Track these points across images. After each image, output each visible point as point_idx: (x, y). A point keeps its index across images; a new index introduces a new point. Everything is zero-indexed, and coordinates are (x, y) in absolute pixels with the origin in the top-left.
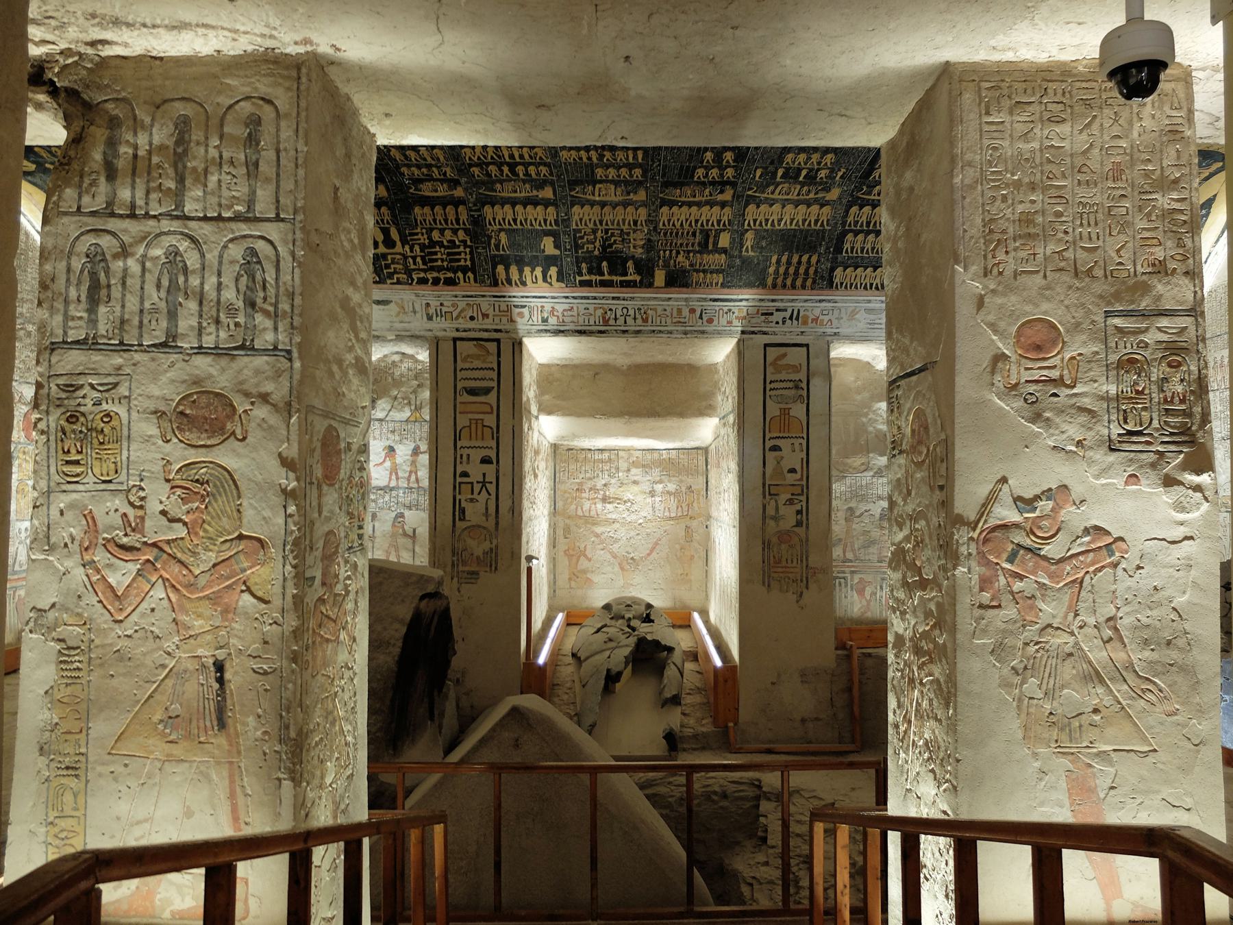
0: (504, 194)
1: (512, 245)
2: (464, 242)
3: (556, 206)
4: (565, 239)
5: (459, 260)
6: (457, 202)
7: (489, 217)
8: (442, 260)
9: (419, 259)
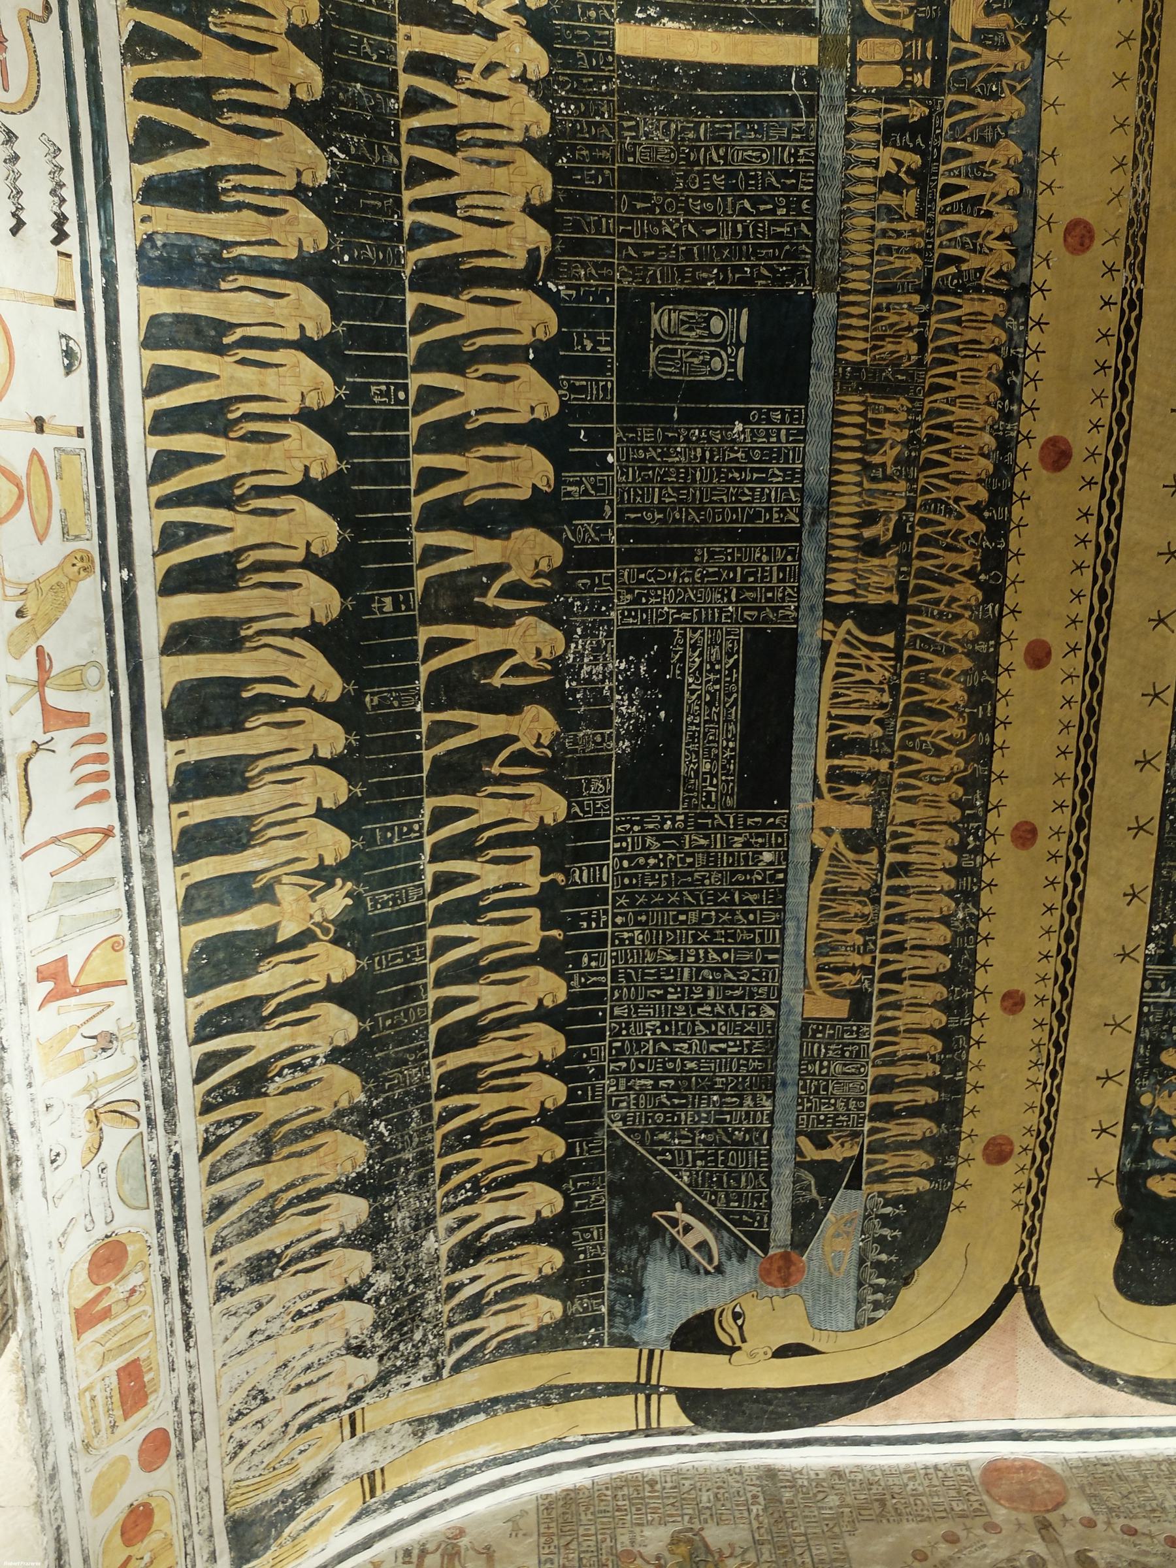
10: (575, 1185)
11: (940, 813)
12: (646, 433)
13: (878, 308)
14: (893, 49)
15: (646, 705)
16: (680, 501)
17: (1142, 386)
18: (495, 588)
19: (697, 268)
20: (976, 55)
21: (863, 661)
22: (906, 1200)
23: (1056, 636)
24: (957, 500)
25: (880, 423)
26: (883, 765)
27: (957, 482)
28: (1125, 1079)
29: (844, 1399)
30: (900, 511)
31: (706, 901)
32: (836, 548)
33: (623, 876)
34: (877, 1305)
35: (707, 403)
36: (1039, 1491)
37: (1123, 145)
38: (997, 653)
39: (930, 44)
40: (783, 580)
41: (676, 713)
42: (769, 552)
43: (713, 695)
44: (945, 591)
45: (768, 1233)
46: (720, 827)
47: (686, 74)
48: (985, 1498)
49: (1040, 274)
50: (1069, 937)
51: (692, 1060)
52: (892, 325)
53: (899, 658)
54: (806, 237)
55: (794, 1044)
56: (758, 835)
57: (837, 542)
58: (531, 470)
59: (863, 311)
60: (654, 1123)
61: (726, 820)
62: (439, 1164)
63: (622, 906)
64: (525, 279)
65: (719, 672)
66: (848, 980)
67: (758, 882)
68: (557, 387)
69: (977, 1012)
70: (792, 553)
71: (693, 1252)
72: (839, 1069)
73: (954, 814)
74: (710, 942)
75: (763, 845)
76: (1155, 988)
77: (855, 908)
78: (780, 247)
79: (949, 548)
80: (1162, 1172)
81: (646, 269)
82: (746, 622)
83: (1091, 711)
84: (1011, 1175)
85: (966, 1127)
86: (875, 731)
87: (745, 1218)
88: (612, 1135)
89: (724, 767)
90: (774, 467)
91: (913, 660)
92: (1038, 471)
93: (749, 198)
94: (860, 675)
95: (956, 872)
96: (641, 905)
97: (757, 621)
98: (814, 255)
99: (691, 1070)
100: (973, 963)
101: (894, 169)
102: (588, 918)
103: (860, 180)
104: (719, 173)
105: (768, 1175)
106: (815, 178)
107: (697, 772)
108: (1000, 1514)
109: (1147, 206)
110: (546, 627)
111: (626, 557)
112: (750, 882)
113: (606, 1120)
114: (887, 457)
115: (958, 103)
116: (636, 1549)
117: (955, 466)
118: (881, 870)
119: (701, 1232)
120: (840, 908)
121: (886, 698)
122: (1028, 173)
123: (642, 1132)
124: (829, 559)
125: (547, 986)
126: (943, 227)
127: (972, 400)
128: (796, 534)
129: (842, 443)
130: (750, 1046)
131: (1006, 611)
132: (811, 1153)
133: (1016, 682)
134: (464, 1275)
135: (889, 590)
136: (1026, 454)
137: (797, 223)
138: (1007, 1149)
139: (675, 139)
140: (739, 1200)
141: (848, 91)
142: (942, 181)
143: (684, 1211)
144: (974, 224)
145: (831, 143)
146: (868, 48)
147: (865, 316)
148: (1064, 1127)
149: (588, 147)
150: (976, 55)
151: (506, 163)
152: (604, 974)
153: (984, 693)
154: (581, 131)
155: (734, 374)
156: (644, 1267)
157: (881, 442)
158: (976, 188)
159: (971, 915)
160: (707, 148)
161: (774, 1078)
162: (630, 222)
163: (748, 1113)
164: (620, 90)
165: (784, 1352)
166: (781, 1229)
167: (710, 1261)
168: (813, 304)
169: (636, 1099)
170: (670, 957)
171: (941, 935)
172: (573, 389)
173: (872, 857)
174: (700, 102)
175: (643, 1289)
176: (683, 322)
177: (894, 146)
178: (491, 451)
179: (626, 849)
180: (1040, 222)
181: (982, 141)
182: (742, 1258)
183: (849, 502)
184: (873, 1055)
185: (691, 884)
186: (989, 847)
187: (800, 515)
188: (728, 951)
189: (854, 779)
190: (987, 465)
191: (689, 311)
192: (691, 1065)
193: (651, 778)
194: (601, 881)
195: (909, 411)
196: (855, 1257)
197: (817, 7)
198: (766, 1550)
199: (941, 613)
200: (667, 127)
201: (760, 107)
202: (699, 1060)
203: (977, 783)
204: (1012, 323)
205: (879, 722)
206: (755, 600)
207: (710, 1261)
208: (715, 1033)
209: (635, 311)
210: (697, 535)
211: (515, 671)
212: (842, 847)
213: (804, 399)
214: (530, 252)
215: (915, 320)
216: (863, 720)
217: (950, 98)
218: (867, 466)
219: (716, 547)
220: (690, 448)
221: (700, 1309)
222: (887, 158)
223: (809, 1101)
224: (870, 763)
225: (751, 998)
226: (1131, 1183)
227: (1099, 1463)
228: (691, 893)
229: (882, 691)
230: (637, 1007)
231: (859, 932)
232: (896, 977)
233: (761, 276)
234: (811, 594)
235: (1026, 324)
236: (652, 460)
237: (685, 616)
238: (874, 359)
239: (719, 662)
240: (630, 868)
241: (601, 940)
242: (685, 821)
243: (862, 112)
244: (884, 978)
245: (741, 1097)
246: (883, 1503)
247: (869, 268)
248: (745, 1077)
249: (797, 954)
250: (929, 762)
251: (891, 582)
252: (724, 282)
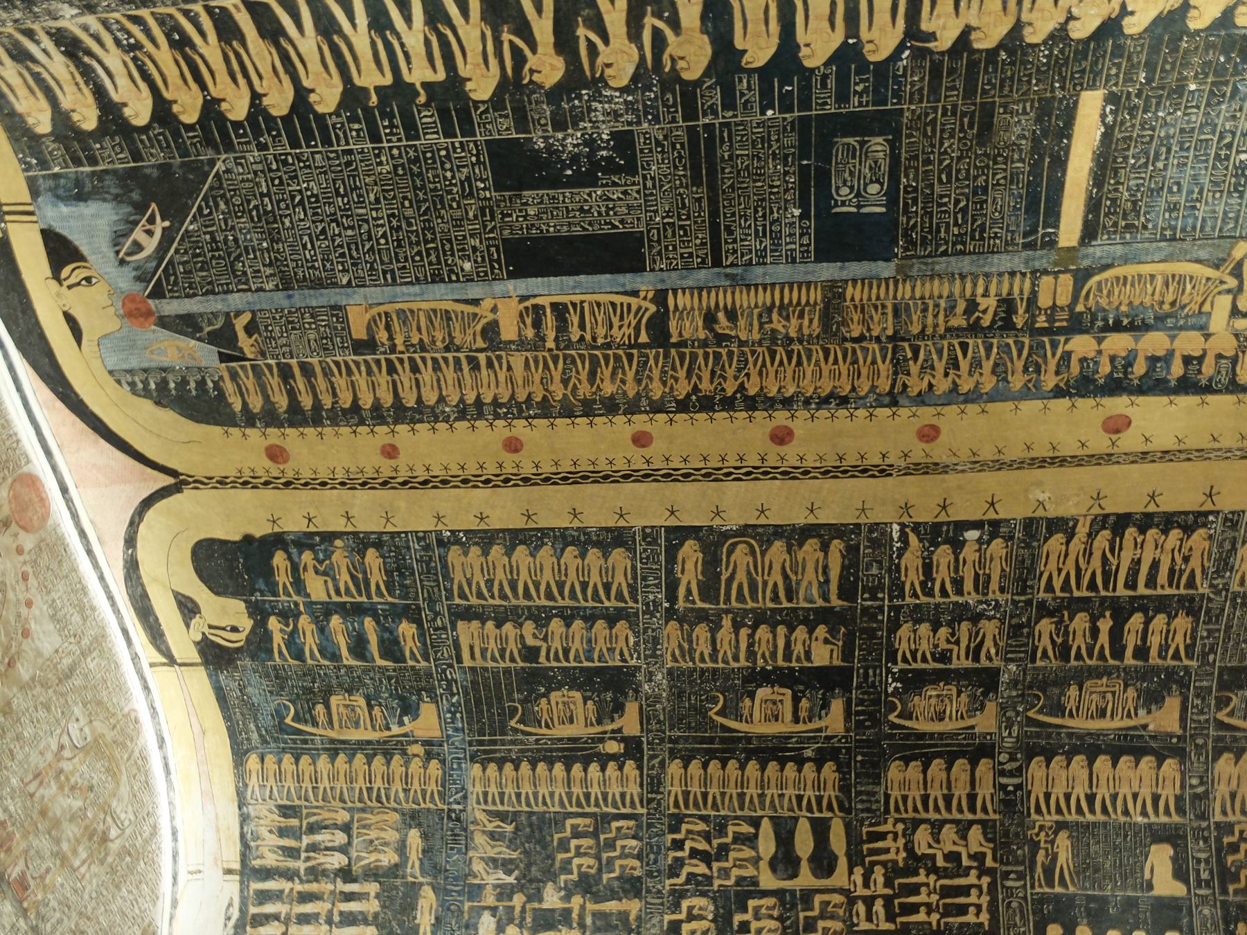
0: (1080, 724)
1: (1086, 868)
2: (979, 857)
3: (1180, 753)
4: (1198, 851)
5: (963, 909)
6: (979, 750)
7: (1038, 791)
8: (930, 909)
9: (879, 906)
10: (159, 134)
11: (521, 388)
12: (792, 139)
13: (884, 306)
14: (1063, 300)
15: (575, 158)
16: (739, 172)
17: (829, 484)
18: (660, 24)
19: (917, 169)
20: (1054, 355)
21: (626, 322)
22: (221, 395)
23: (656, 451)
24: (748, 375)
25: (801, 316)
26: (550, 344)
27: (760, 373)
28: (350, 529)
29: (48, 369)
30: (737, 337)
31: (424, 221)
32: (709, 293)
33: (432, 152)
34: (132, 385)
35: (814, 186)
36: (30, 514)
37: (987, 454)
38: (641, 412)
39: (1065, 324)
40: (682, 257)
41: (573, 183)
42: (703, 244)
43: (589, 211)
44: (682, 374)
45: (165, 297)
46: (485, 227)
47: (1061, 149)
48: (10, 480)
49: (904, 412)
50: (444, 482)
51: (291, 222)
52: (871, 318)
53: (631, 346)
54: (936, 250)
55: (323, 301)
56: (483, 257)
57: (713, 294)
58: (758, 48)
59: (882, 296)
60: (232, 197)
61: (491, 231)
62: (144, 13)
63: (407, 153)
64: (913, 32)
65: (608, 214)
66: (382, 336)
67: (446, 261)
68: (826, 64)
69: (377, 429)
70: (703, 262)
71: (131, 239)
72: (312, 337)
73: (521, 397)
74: (391, 228)
75: (476, 262)
76: (419, 539)
77: (439, 336)
78: (930, 232)
79: (713, 373)
80: (290, 558)
81: (918, 129)
82: (649, 232)
83: (606, 477)
84: (263, 466)
85: (288, 431)
86: (575, 334)
87: (172, 278)
88: (212, 163)
89: (533, 225)
90: (767, 242)
91: (630, 357)
92: (770, 426)
93: (967, 205)
94: (616, 321)
95: (479, 403)
96: (411, 169)
97: (650, 240)
98: (924, 257)
99: (283, 223)
100: (413, 421)
101: (981, 308)
102: (392, 126)
103: (975, 285)
104: (986, 181)
105: (213, 292)
106: (979, 253)
107: (526, 204)
109: (946, 472)
110: (631, 70)
111: (692, 131)
112: (445, 255)
113: (224, 156)
114: (777, 323)
115: (1023, 347)
117: (772, 371)
118: (471, 351)
119: (150, 245)
120: (437, 325)
121: (600, 341)
122: (973, 397)
123: (221, 187)
124: (700, 289)
125: (327, 97)
126: (939, 346)
127: (818, 377)
128: (717, 263)
129: (786, 291)
130: (313, 267)
131: (671, 415)
132: (240, 323)
133: (621, 427)
134: (47, 43)
135: (680, 335)
136: (781, 417)
137: (947, 243)
138: (280, 460)
139: (1014, 144)
140: (185, 272)
141: (1038, 271)
142: (971, 341)
143: (164, 229)
144: (940, 366)
145: (1003, 262)
146: (1067, 280)
147: (878, 298)
148: (305, 494)
149: (1013, 75)
150: (1054, 355)
151: (1005, 9)
152: (347, 143)
153: (611, 407)
154: (1026, 69)
155: (836, 205)
156: (104, 200)
157: (787, 318)
158: (964, 365)
159: (449, 416)
160: (1005, 170)
161: (293, 289)
162: (954, 114)
163: (259, 271)
164: (1054, 98)
165: (70, 319)
166: (172, 307)
167: (128, 254)
168: (887, 260)
169: (248, 180)
170: (372, 197)
171: (430, 398)
172: (825, 77)
173: (480, 343)
174: (1042, 158)
175: (85, 201)
176: (876, 162)
177: (998, 306)
178: (773, 12)
179: (455, 152)
180: (939, 408)
181: (996, 365)
182: (138, 279)
183: (743, 299)
184: (328, 360)
185: (435, 209)
186: (500, 423)
187: (732, 265)
188: (387, 243)
189: (537, 324)
190: (773, 391)
191: (885, 167)
192: (287, 222)
193: (516, 167)
194: (425, 134)
195: (810, 335)
196: (166, 365)
197: (1099, 242)
199: (666, 372)
200: (1024, 137)
201: (1032, 208)
202: (293, 228)
203: (546, 409)
204: (872, 397)
205: (582, 338)
206: (666, 237)
207: (128, 254)
208: (318, 239)
209: (886, 124)
210: (713, 187)
211: (592, 46)
212: (484, 321)
213: (818, 260)
214: (934, 33)
215: (875, 334)
216: (582, 326)
217: (1027, 341)
218: (769, 310)
219: (705, 203)
220: (780, 176)
221: (84, 250)
222: (990, 303)
223: (281, 317)
224: (551, 335)
225: (353, 264)
226: (277, 541)
228: (428, 208)
229: (606, 337)
230: (325, 173)
231: (421, 340)
232: (392, 370)
233: (909, 219)
234: (673, 279)
235: (871, 406)
236: (770, 146)
237: (649, 184)
238: (848, 307)
239: (615, 214)
240: (440, 157)
241: (375, 138)
242: (485, 199)
243: (1023, 282)
244: (390, 363)
245: (270, 265)
247: (913, 298)
248: (287, 266)
249: (395, 296)
250: (557, 376)
251: (686, 335)
252: (906, 192)
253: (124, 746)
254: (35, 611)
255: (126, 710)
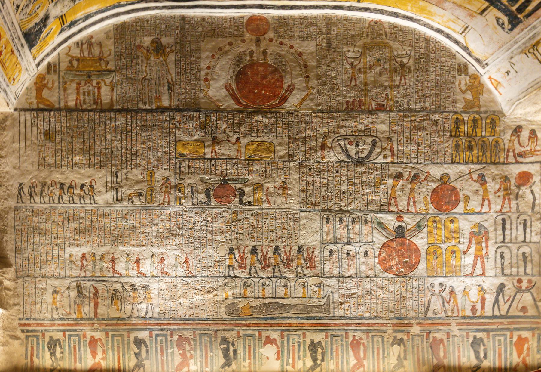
36: (261, 28)
48: (245, 30)
108: (247, 36)
116: (142, 44)
198: (178, 46)
227: (284, 18)
246: (214, 30)
253: (379, 35)
254: (296, 46)
255: (367, 25)
